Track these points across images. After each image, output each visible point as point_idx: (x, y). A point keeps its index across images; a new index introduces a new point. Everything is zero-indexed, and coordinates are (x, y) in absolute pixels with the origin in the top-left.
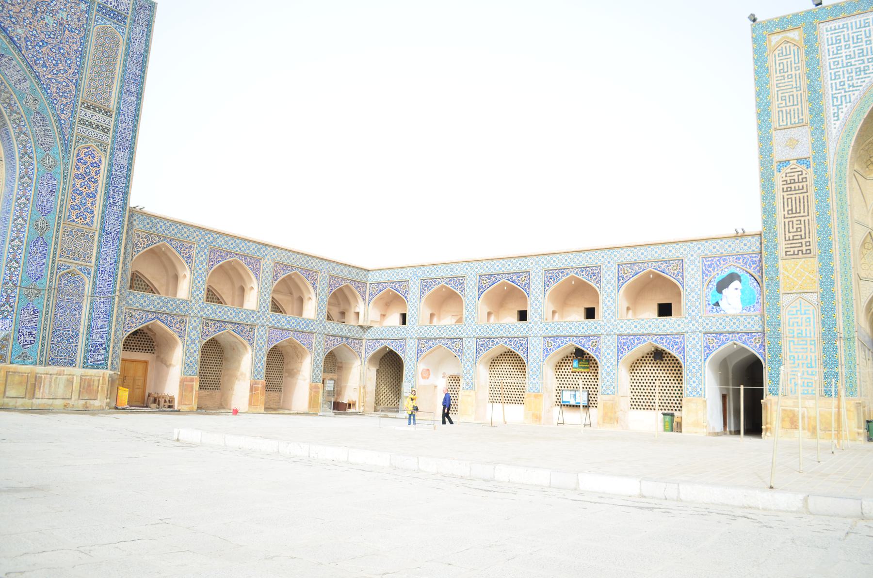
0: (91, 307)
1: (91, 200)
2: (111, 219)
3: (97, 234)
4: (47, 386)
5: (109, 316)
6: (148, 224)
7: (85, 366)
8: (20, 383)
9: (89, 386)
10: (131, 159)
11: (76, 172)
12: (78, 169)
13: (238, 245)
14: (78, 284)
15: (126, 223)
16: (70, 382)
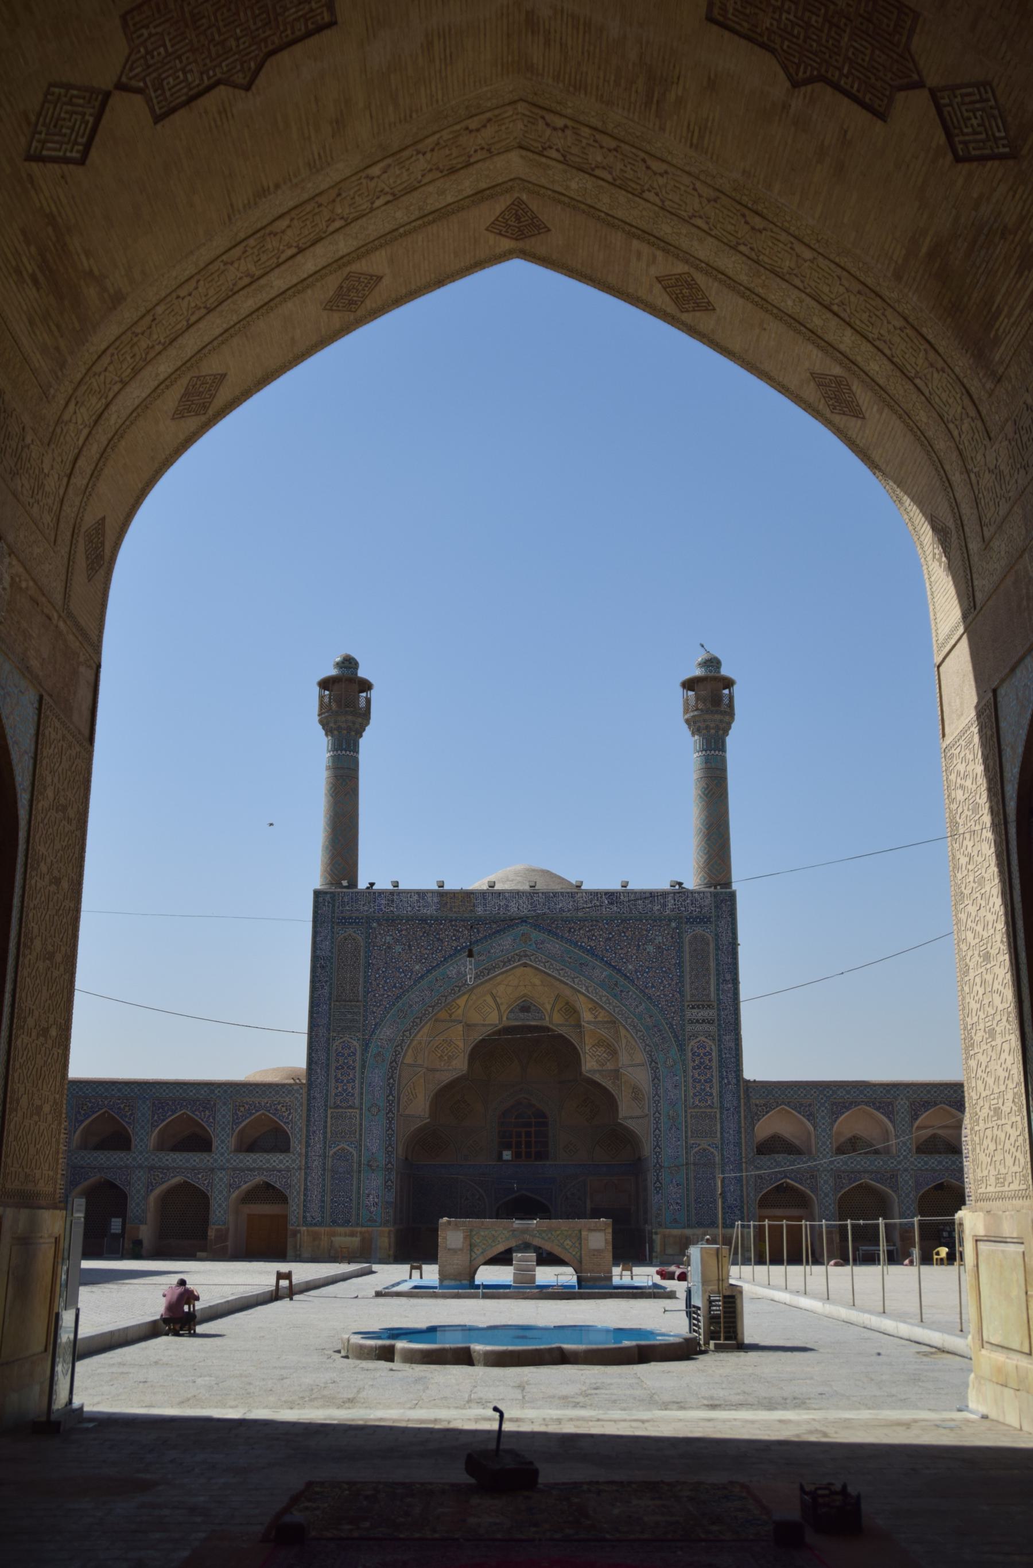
1: (708, 1085)
12: (694, 1061)
13: (861, 1092)
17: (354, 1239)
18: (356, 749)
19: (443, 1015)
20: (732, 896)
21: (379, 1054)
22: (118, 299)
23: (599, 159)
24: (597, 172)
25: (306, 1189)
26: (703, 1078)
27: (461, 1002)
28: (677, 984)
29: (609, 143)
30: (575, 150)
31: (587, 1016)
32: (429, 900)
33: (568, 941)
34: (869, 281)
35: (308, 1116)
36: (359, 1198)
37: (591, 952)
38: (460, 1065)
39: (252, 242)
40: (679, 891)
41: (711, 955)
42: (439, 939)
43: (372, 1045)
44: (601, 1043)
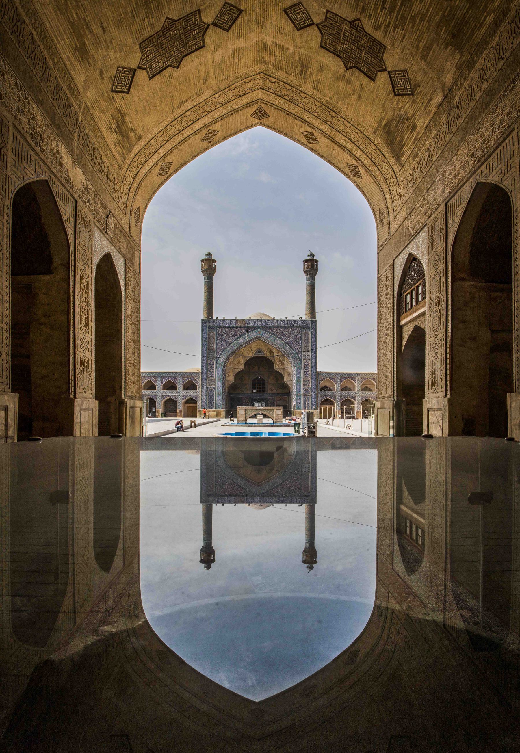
2: (314, 376)
7: (312, 409)
18: (212, 280)
19: (237, 353)
20: (316, 321)
21: (220, 364)
22: (140, 137)
23: (285, 92)
24: (285, 97)
27: (242, 350)
29: (289, 87)
30: (278, 90)
31: (276, 354)
33: (272, 334)
34: (366, 134)
37: (277, 336)
38: (242, 367)
39: (179, 119)
40: (301, 320)
44: (280, 361)
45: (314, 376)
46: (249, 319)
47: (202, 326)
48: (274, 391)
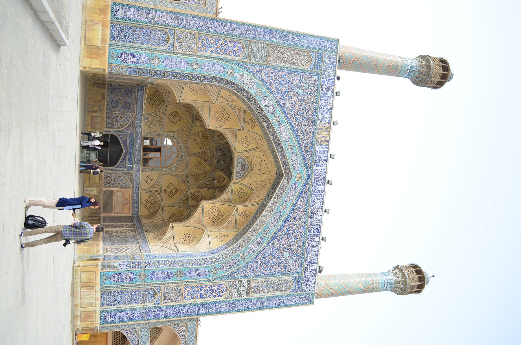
0: (137, 309)
1: (199, 296)
2: (190, 309)
3: (180, 303)
4: (88, 293)
5: (133, 320)
6: (192, 330)
7: (101, 312)
8: (89, 279)
9: (89, 316)
10: (227, 312)
11: (213, 285)
12: (214, 286)
14: (150, 299)
15: (190, 318)
16: (91, 305)
17: (100, 42)
20: (311, 302)
25: (140, 8)
26: (203, 292)
28: (263, 273)
31: (240, 209)
32: (327, 115)
35: (194, 16)
36: (131, 48)
37: (288, 219)
38: (212, 125)
41: (279, 293)
42: (303, 120)
43: (239, 68)
45: (190, 309)
46: (330, 153)
47: (326, 39)
48: (143, 186)
